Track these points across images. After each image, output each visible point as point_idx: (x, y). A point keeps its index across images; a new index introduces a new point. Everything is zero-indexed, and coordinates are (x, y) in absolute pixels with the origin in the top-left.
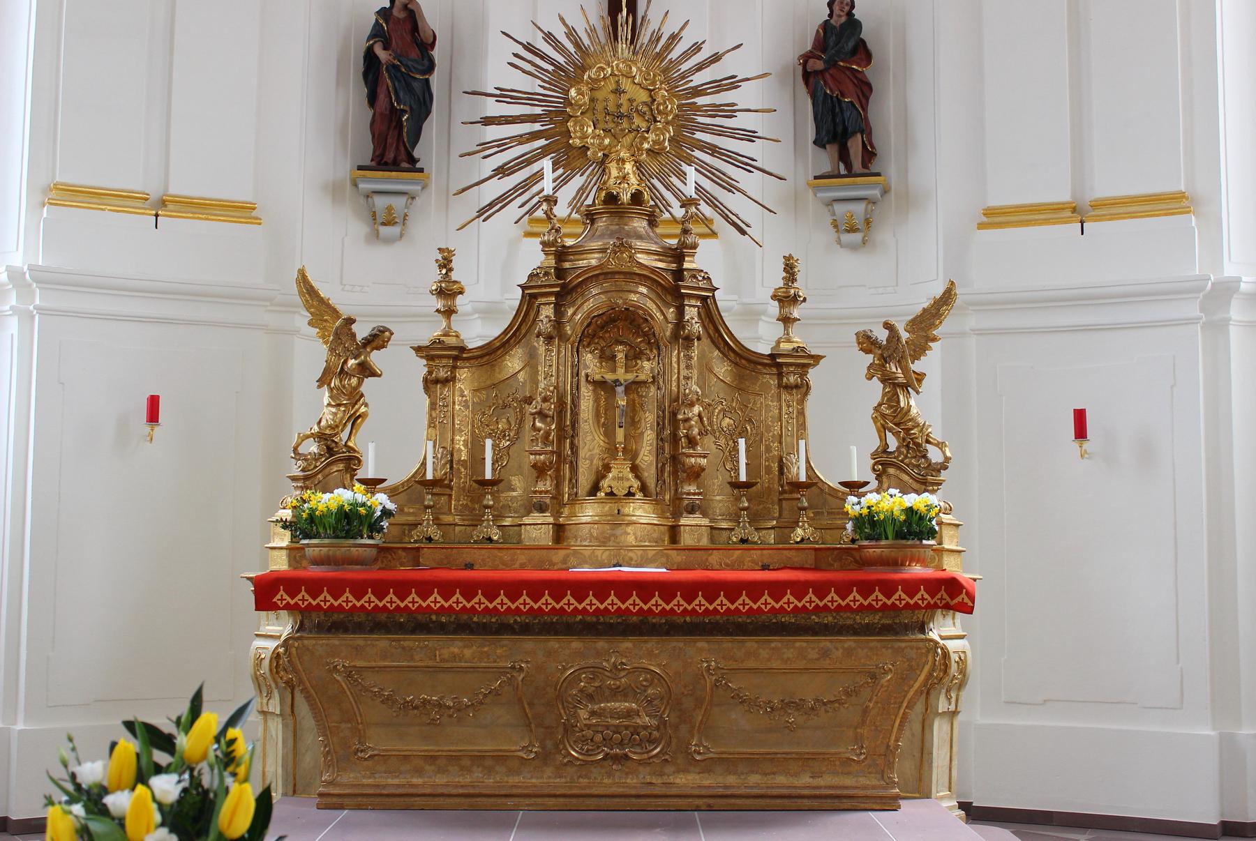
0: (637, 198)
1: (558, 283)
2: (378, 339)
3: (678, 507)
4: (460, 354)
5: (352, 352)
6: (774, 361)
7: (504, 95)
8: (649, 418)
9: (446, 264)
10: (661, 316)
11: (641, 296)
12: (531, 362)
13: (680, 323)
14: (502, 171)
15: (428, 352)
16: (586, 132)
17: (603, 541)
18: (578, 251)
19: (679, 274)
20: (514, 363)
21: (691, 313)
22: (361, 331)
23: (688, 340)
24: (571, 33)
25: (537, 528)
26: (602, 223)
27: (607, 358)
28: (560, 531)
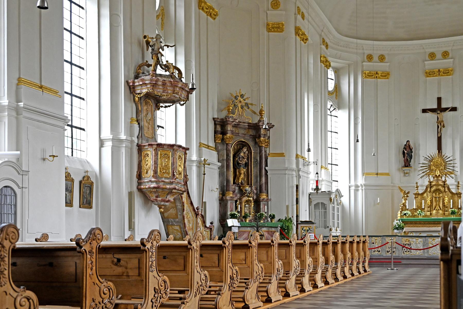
0: (439, 175)
1: (431, 185)
2: (408, 193)
3: (445, 211)
4: (419, 194)
5: (406, 194)
6: (457, 194)
7: (423, 164)
8: (441, 201)
9: (417, 184)
10: (442, 189)
11: (440, 187)
12: (427, 195)
13: (445, 190)
14: (423, 173)
15: (415, 194)
16: (433, 167)
17: (436, 215)
18: (432, 182)
19: (444, 184)
20: (425, 195)
21: (446, 189)
22: (406, 192)
23: (446, 192)
24: (431, 156)
25: (428, 213)
26: (435, 178)
27: (436, 194)
28: (431, 214)
